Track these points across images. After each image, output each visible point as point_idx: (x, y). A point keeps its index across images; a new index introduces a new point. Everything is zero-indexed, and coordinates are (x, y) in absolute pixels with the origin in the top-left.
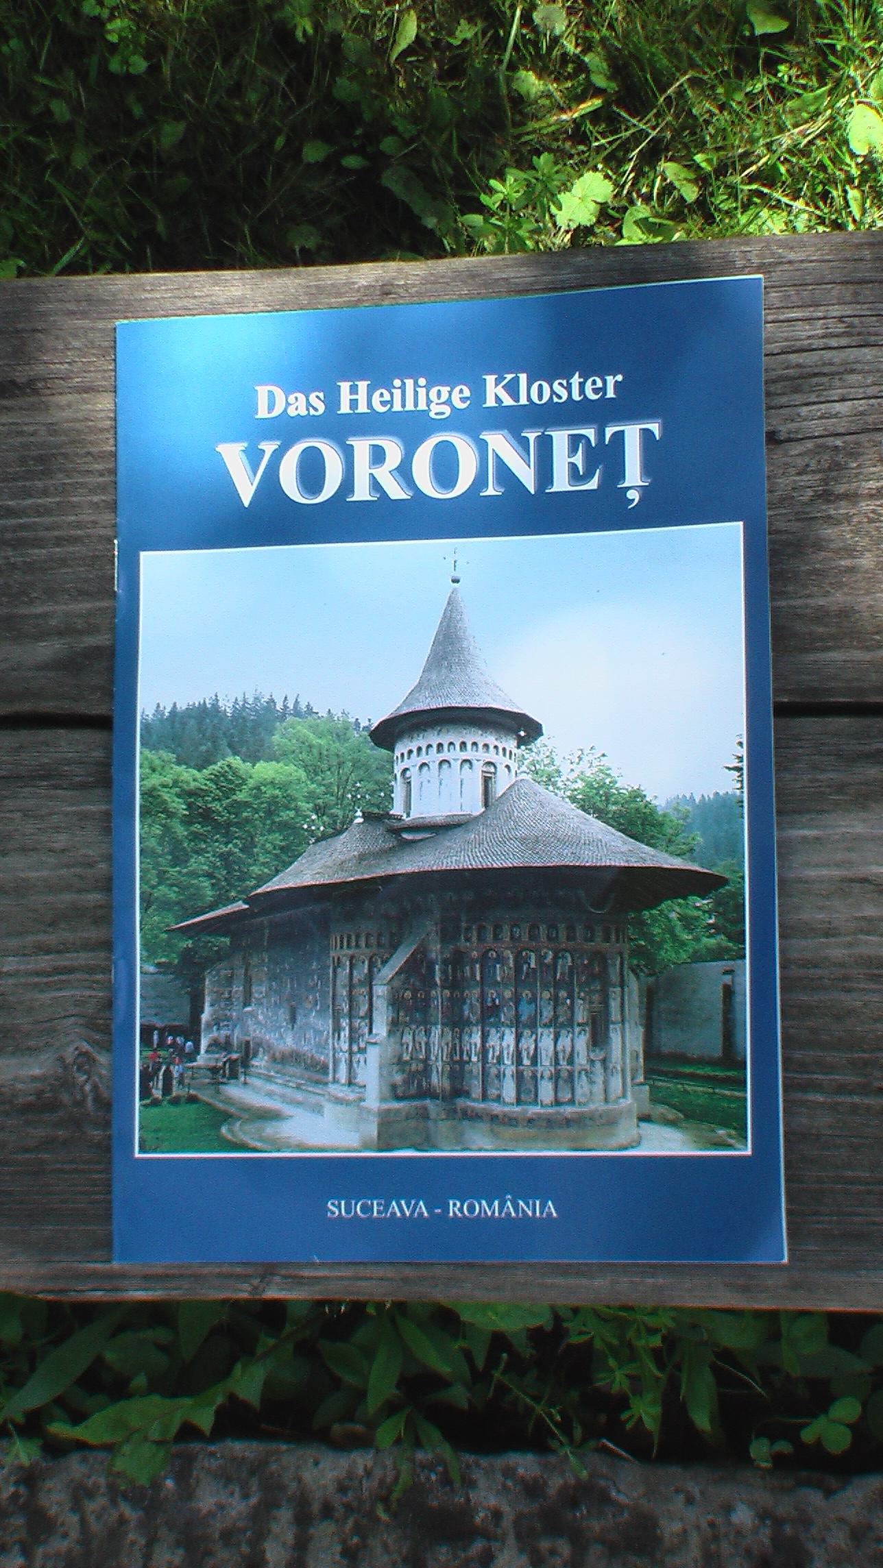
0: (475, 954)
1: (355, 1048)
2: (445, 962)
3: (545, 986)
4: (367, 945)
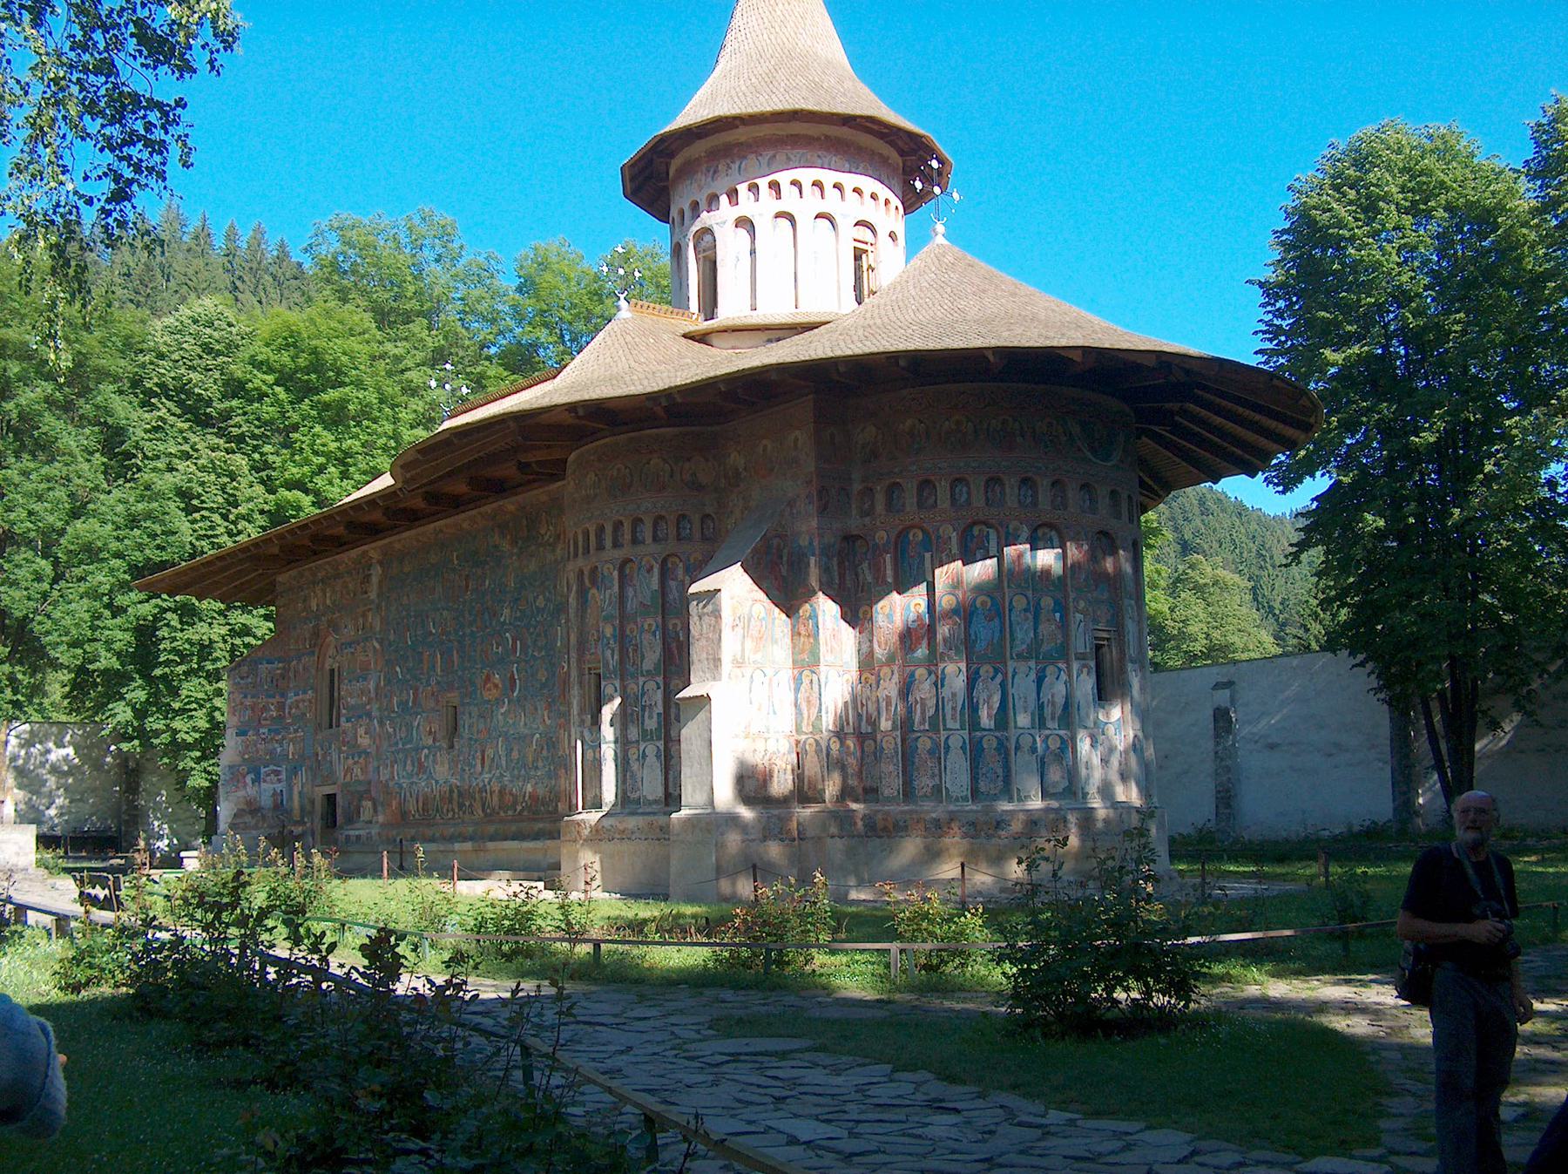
1: (633, 733)
2: (826, 552)
4: (655, 539)
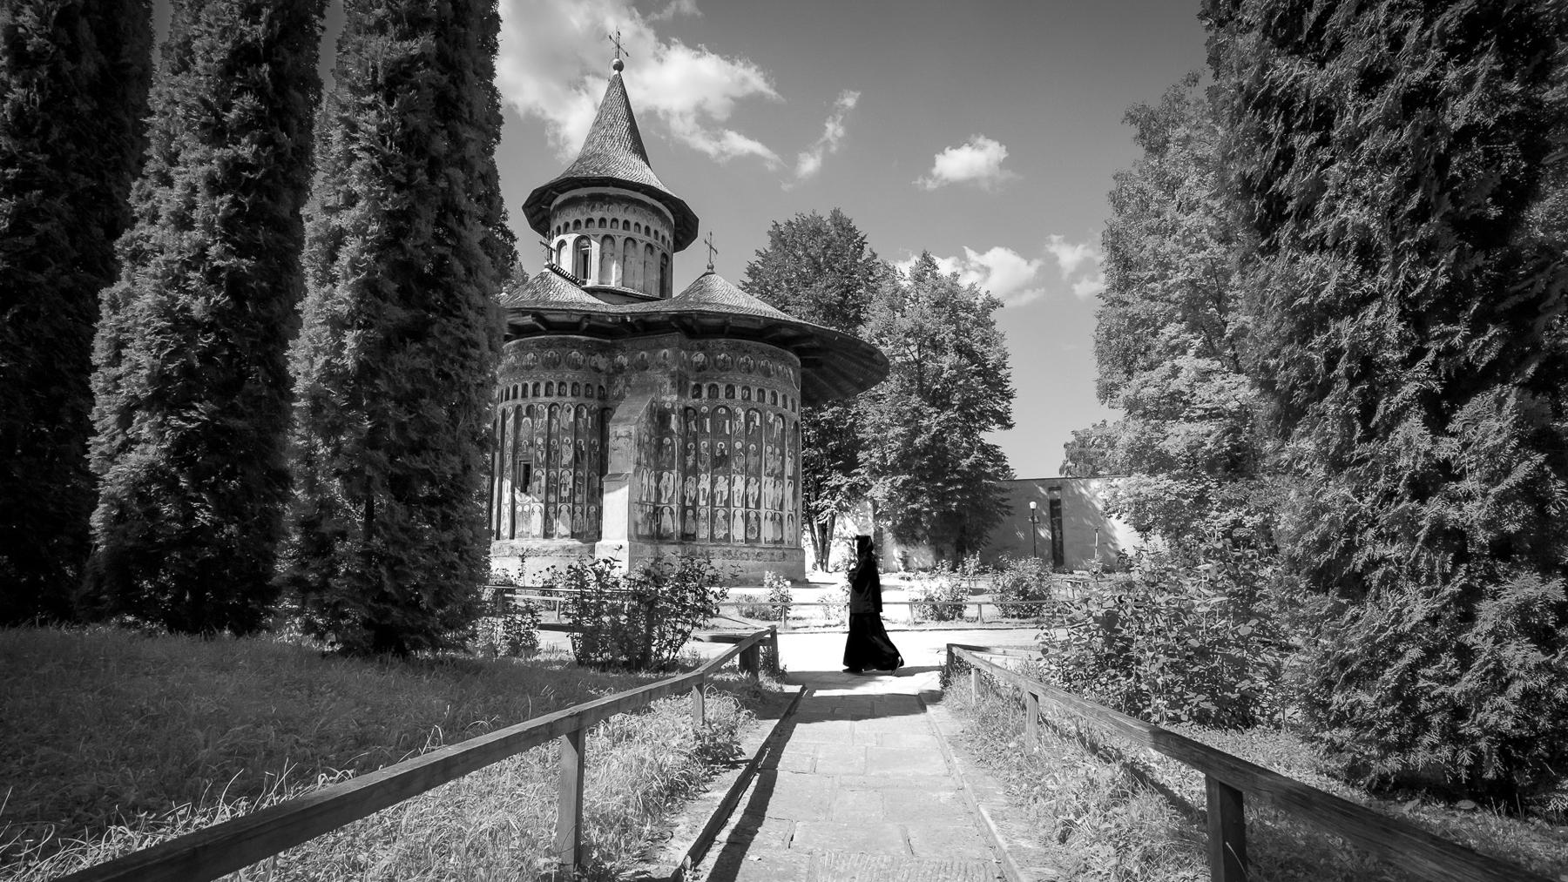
0: (705, 409)
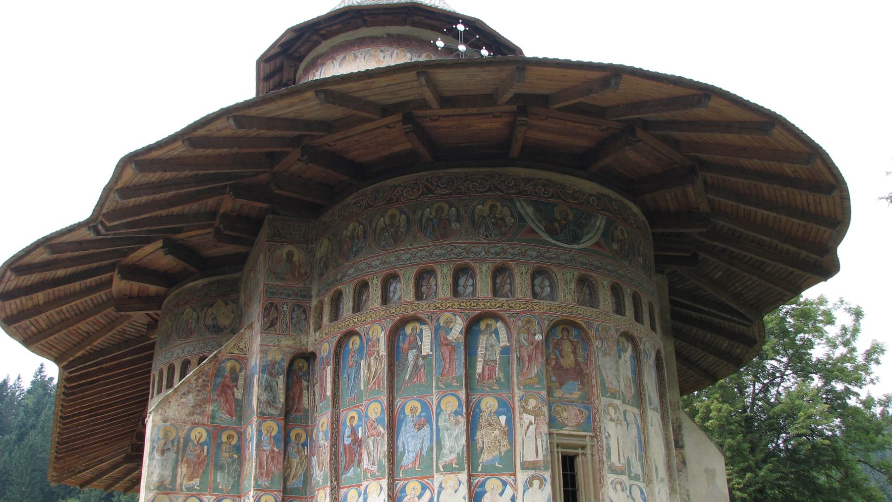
2: (269, 369)
3: (447, 390)
